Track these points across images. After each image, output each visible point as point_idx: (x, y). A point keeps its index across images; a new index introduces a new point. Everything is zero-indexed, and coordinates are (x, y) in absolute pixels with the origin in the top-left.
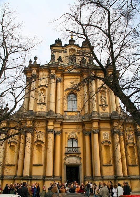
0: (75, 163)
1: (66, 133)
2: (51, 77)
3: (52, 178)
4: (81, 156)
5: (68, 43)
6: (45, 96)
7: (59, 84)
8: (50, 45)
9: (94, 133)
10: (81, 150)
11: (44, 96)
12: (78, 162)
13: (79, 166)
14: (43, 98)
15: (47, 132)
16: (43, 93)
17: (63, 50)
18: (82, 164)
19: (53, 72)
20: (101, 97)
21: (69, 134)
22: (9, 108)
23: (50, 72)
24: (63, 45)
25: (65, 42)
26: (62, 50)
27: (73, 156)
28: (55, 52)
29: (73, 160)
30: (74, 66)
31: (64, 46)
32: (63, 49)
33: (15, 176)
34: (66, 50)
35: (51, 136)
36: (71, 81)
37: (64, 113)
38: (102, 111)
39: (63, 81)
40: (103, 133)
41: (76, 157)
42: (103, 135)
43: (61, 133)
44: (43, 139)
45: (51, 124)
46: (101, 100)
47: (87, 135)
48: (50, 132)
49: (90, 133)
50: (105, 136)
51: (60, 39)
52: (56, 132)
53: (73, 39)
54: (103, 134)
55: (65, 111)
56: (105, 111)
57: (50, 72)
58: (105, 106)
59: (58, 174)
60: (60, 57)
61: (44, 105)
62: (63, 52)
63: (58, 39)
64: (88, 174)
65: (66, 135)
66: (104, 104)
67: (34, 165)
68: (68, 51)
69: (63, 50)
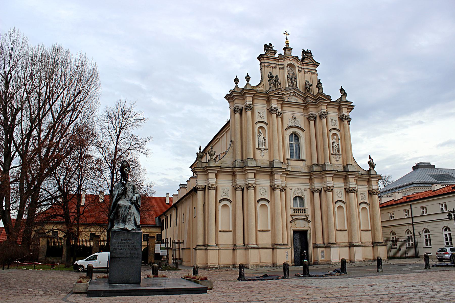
0: (303, 227)
1: (291, 189)
2: (271, 111)
4: (310, 219)
10: (309, 212)
11: (263, 137)
12: (307, 227)
13: (307, 231)
14: (263, 142)
16: (261, 133)
17: (279, 65)
19: (274, 104)
20: (333, 143)
21: (293, 190)
23: (269, 101)
25: (279, 49)
26: (277, 64)
27: (300, 219)
29: (301, 225)
30: (296, 93)
33: (235, 245)
34: (283, 64)
37: (286, 161)
38: (336, 163)
40: (335, 191)
41: (304, 220)
42: (336, 194)
44: (267, 197)
45: (277, 177)
46: (333, 147)
47: (317, 192)
54: (336, 191)
55: (287, 160)
57: (269, 101)
60: (276, 76)
64: (320, 241)
67: (259, 231)
68: (285, 66)
69: (278, 63)
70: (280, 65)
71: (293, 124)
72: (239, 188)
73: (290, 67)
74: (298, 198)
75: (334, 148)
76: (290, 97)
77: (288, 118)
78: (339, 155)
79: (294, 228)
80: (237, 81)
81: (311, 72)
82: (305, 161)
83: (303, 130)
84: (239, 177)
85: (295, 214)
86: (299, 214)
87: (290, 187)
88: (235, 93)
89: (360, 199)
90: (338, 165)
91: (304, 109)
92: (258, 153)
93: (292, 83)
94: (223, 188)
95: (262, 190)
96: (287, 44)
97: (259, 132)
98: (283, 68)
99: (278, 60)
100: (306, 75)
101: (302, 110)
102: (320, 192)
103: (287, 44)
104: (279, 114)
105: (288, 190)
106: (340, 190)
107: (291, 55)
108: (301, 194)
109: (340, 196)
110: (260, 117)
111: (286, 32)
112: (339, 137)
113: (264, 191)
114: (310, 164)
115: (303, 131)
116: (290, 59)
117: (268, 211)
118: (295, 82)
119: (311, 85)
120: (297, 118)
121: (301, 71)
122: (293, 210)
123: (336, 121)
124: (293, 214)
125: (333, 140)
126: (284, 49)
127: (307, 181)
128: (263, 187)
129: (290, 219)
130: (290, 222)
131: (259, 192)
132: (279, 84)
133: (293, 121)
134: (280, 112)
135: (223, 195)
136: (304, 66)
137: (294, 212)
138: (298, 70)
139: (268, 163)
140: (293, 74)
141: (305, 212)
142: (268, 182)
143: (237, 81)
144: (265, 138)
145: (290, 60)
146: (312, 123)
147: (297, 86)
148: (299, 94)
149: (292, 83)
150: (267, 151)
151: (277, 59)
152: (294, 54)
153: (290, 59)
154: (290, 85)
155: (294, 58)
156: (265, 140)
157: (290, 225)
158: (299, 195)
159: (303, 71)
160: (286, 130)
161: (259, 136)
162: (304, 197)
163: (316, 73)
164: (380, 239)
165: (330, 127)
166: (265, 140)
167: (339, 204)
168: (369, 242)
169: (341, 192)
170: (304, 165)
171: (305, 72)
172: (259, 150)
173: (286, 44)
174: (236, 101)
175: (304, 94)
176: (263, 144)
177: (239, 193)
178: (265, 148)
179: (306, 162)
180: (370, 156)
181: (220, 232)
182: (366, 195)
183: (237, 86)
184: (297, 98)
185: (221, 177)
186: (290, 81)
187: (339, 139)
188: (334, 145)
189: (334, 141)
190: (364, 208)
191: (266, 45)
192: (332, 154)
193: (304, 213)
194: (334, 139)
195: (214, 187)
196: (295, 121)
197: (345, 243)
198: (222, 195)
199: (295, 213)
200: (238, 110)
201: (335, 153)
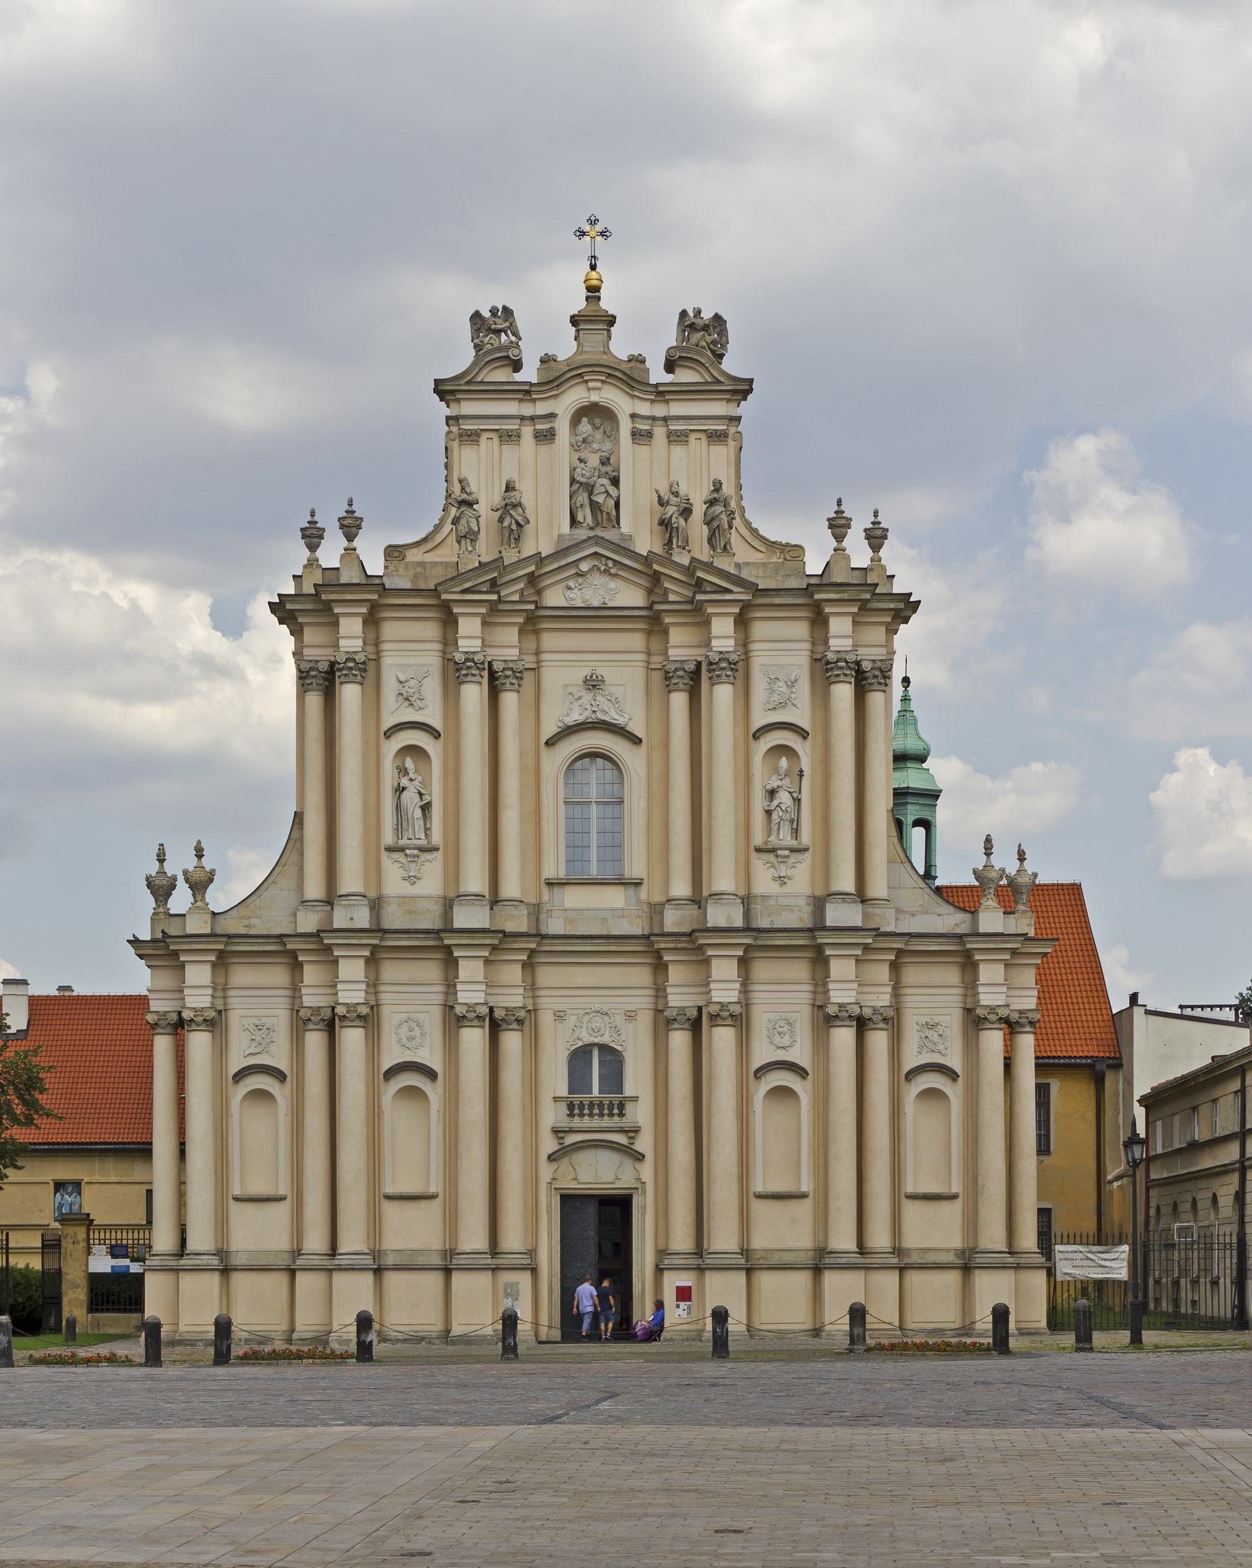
0: (610, 1178)
1: (559, 1016)
3: (489, 1261)
4: (644, 1144)
5: (565, 347)
6: (430, 795)
7: (509, 700)
8: (437, 382)
9: (714, 1018)
10: (641, 1114)
11: (421, 794)
14: (418, 813)
15: (454, 1020)
16: (412, 775)
18: (644, 1192)
21: (572, 1020)
22: (212, 872)
24: (529, 373)
26: (522, 418)
27: (596, 1147)
28: (471, 437)
30: (608, 558)
31: (535, 381)
32: (534, 400)
33: (297, 1253)
34: (552, 416)
35: (474, 1039)
36: (588, 672)
37: (545, 890)
38: (774, 888)
39: (536, 670)
40: (761, 1019)
42: (765, 1032)
43: (526, 1020)
45: (470, 969)
46: (769, 813)
48: (471, 1020)
49: (695, 1013)
50: (779, 1033)
51: (504, 307)
52: (503, 1013)
53: (607, 303)
55: (550, 884)
56: (790, 888)
58: (787, 853)
59: (513, 1239)
60: (509, 488)
61: (428, 856)
62: (527, 432)
63: (494, 311)
64: (682, 1240)
65: (559, 1026)
66: (784, 837)
67: (389, 1197)
68: (562, 427)
69: (527, 410)
70: (540, 417)
71: (587, 713)
72: (309, 1019)
73: (597, 421)
74: (596, 1053)
75: (775, 816)
76: (580, 580)
77: (566, 686)
78: (793, 850)
79: (569, 1185)
80: (312, 536)
81: (705, 431)
82: (638, 884)
83: (637, 741)
84: (312, 974)
85: (577, 1122)
86: (596, 1123)
87: (558, 1007)
88: (293, 602)
89: (916, 1049)
90: (782, 901)
91: (649, 633)
92: (393, 870)
93: (594, 506)
94: (249, 1022)
95: (405, 1027)
96: (593, 291)
97: (403, 771)
98: (546, 437)
99: (528, 392)
100: (678, 450)
101: (636, 641)
102: (695, 1026)
103: (593, 291)
104: (507, 677)
105: (546, 1018)
106: (789, 1015)
107: (606, 351)
108: (607, 1035)
109: (786, 1041)
110: (406, 703)
111: (593, 222)
112: (805, 764)
113: (417, 1032)
114: (658, 898)
115: (636, 743)
116: (586, 382)
117: (429, 1116)
118: (612, 503)
119: (686, 512)
120: (608, 680)
121: (649, 435)
122: (563, 1108)
123: (792, 684)
124: (565, 1122)
125: (775, 777)
126: (575, 321)
127: (641, 976)
128: (412, 1015)
129: (549, 1144)
130: (551, 1158)
131: (394, 1036)
132: (518, 524)
133: (587, 697)
134: (510, 665)
135: (252, 1050)
136: (667, 402)
137: (571, 1115)
138: (636, 435)
139: (437, 909)
140: (605, 462)
141: (621, 1115)
142: (435, 995)
143: (312, 536)
144: (427, 798)
145: (590, 384)
146: (679, 700)
147: (618, 523)
148: (620, 563)
149: (594, 506)
150: (435, 854)
151: (526, 393)
152: (621, 346)
153: (586, 382)
154: (580, 518)
155: (610, 375)
156: (426, 808)
157: (546, 1171)
158: (596, 1040)
159: (660, 432)
160: (547, 743)
161: (400, 790)
162: (619, 1048)
163: (732, 430)
164: (993, 1236)
165: (760, 718)
166: (426, 808)
167: (784, 1078)
168: (948, 1250)
169: (790, 1024)
170: (638, 901)
171: (677, 438)
172: (396, 855)
173: (589, 289)
174: (309, 635)
175: (647, 560)
176: (419, 824)
177: (315, 1041)
178: (423, 842)
179: (644, 888)
180: (988, 841)
181: (235, 1202)
182: (948, 1032)
183: (312, 563)
184: (613, 584)
185: (242, 975)
186: (583, 498)
187: (801, 771)
188: (775, 803)
189: (774, 783)
190: (931, 1094)
191: (476, 316)
192: (758, 850)
193: (616, 1118)
194: (776, 771)
195: (205, 1020)
196: (599, 698)
197: (795, 1254)
198: (247, 1053)
199: (577, 1119)
200: (314, 677)
201: (770, 846)
